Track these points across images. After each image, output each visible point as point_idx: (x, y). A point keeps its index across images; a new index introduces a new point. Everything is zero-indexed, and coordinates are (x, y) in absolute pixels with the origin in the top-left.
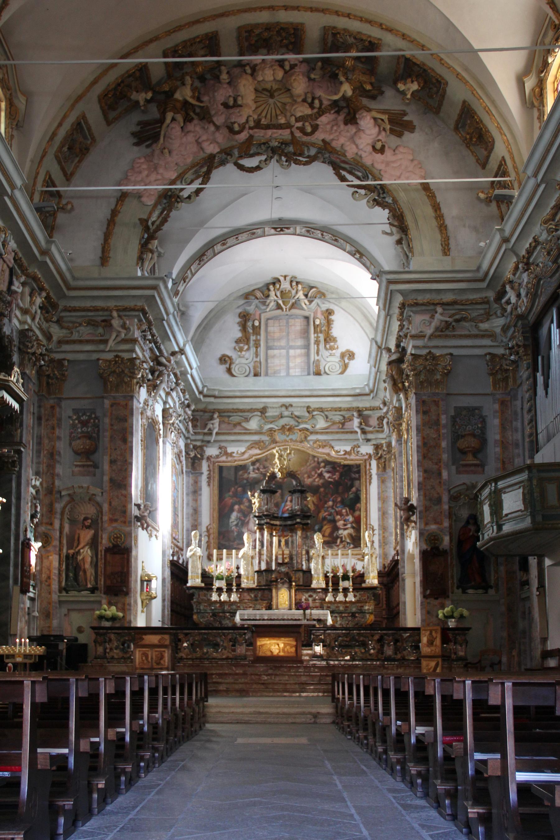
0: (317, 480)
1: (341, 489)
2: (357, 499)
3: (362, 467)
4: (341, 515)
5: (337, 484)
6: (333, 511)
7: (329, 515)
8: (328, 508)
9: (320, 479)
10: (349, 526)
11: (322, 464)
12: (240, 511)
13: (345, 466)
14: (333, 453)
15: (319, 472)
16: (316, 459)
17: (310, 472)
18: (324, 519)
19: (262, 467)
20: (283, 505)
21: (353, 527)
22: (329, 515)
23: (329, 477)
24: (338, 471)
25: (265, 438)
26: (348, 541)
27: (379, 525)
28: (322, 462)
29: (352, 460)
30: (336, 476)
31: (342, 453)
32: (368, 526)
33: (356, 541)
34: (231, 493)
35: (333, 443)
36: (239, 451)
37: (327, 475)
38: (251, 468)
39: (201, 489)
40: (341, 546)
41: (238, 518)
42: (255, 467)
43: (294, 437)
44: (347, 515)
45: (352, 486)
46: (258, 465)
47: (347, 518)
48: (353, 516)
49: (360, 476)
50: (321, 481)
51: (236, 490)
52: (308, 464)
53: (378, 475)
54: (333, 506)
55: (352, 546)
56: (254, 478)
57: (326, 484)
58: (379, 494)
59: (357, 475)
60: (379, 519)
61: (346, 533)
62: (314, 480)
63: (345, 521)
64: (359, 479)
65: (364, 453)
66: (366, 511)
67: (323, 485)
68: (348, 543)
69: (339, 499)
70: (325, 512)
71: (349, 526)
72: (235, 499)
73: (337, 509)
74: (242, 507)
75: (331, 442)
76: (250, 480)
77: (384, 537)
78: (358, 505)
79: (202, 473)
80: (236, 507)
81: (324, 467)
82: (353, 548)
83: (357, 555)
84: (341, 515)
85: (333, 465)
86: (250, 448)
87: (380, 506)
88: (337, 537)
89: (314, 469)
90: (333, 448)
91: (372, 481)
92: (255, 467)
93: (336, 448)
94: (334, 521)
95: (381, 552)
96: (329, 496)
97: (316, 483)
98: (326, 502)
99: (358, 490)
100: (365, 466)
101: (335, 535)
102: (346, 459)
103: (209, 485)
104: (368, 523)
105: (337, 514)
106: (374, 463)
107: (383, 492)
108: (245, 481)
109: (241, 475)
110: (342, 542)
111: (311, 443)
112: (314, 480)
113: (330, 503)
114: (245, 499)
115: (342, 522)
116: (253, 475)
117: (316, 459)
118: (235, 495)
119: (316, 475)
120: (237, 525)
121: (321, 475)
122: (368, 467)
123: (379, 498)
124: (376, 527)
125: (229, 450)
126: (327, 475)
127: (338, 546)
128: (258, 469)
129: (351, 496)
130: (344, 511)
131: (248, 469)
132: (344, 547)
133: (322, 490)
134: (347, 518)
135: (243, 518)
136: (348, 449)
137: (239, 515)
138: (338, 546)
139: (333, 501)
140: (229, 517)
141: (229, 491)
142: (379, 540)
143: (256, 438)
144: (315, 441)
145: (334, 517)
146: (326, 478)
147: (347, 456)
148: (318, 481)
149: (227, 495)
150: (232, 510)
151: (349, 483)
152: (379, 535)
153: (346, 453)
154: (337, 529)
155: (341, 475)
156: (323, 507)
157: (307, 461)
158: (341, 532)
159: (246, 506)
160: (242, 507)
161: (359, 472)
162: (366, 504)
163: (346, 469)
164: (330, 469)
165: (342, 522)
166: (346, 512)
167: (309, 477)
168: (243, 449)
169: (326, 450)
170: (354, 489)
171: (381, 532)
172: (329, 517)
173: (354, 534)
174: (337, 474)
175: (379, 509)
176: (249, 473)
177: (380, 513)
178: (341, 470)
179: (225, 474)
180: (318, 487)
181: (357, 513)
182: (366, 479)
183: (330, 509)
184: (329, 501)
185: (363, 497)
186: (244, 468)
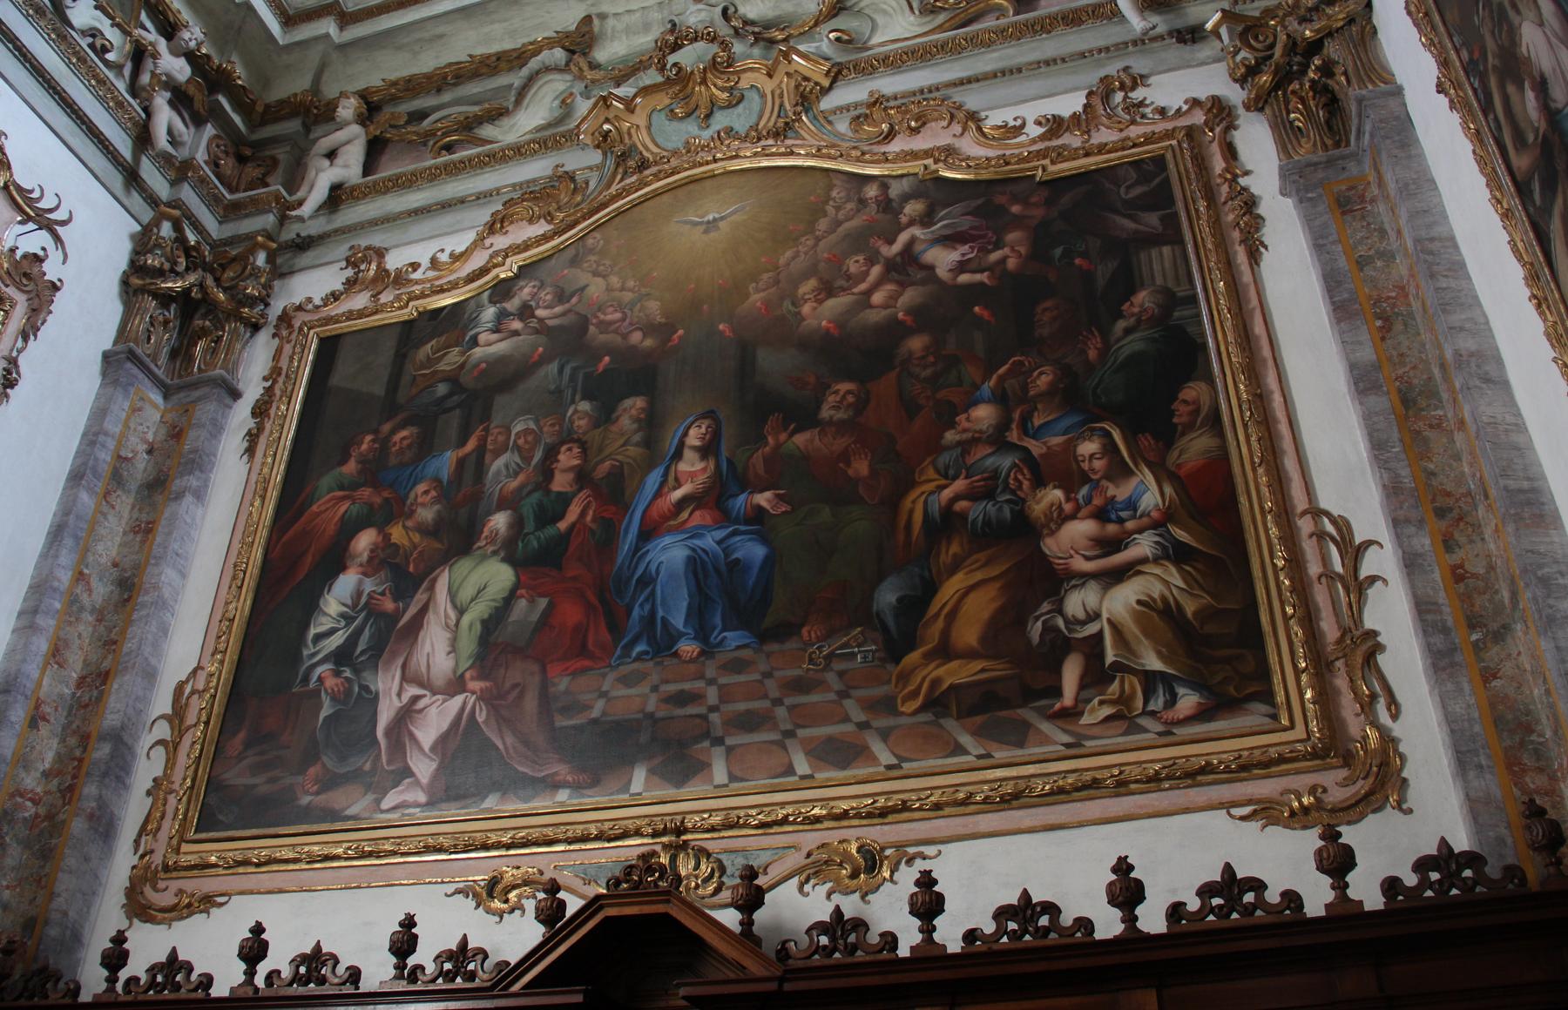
0: (877, 298)
1: (1046, 315)
2: (1181, 354)
3: (1185, 189)
4: (1070, 476)
5: (1015, 295)
6: (1006, 461)
7: (972, 495)
8: (966, 446)
9: (903, 285)
10: (1144, 545)
11: (913, 208)
12: (385, 560)
13: (1057, 185)
14: (971, 147)
15: (897, 247)
16: (872, 191)
17: (837, 262)
18: (945, 523)
19: (547, 296)
20: (653, 479)
21: (1176, 554)
22: (972, 495)
23: (962, 267)
24: (1017, 222)
25: (582, 160)
26: (1154, 663)
27: (1392, 491)
28: (906, 198)
29: (1102, 149)
30: (1012, 251)
31: (1034, 131)
32: (1305, 525)
33: (1220, 652)
34: (351, 467)
35: (971, 99)
36: (438, 247)
37: (943, 259)
38: (490, 313)
39: (199, 463)
40: (1097, 713)
41: (361, 608)
42: (512, 305)
43: (739, 119)
44: (1119, 471)
45: (1127, 283)
46: (526, 291)
47: (1121, 492)
48: (1162, 472)
49: (1172, 221)
50: (910, 296)
51: (384, 443)
52: (823, 225)
53: (1296, 179)
54: (1003, 426)
55: (1188, 701)
56: (502, 360)
57: (945, 309)
58: (1332, 282)
59: (1153, 220)
60: (1377, 446)
61: (1122, 601)
62: (865, 300)
63: (1101, 515)
64: (1171, 234)
65: (1174, 101)
66: (1266, 422)
67: (922, 318)
68: (1150, 680)
69: (1043, 380)
70: (948, 476)
71: (1144, 545)
72: (366, 492)
73: (1036, 448)
74: (397, 533)
75: (958, 96)
76: (466, 379)
77: (1458, 575)
78: (1193, 391)
79: (236, 395)
80: (365, 541)
81: (926, 220)
82: (1202, 715)
83: (1245, 768)
84: (1070, 476)
85: (984, 202)
86: (496, 225)
87: (1367, 354)
88: (1059, 645)
89: (859, 242)
90: (974, 118)
91: (1268, 234)
92: (512, 305)
93: (994, 118)
94: (1023, 531)
95: (1468, 701)
96: (971, 372)
97: (874, 316)
98: (948, 415)
99: (1178, 301)
100: (1201, 163)
101: (1035, 630)
102: (1060, 154)
103: (250, 451)
104: (1300, 502)
105: (1039, 482)
106: (1257, 143)
107: (1361, 263)
108: (442, 389)
109: (430, 361)
110: (1096, 676)
111: (843, 126)
112: (865, 300)
113: (984, 415)
114: (421, 488)
115: (1081, 529)
116: (490, 347)
117: (872, 191)
118: (373, 472)
119: (876, 271)
120: (342, 657)
121: (906, 266)
122: (1218, 164)
123: (1342, 310)
124: (1366, 512)
125: (394, 261)
126: (943, 259)
127: (1069, 715)
128: (526, 312)
129: (1133, 345)
130: (1088, 447)
131: (474, 320)
132: (1123, 717)
133: (916, 344)
134: (1121, 492)
135: (389, 605)
136: (1070, 104)
137: (369, 586)
138: (1069, 715)
139: (1001, 398)
140: (311, 607)
141: (343, 462)
142: (1423, 608)
143: (536, 169)
144: (862, 115)
145: (1019, 505)
146: (942, 272)
147: (1073, 140)
148: (887, 301)
149: (326, 481)
150: (335, 562)
151: (1103, 272)
152: (1411, 564)
153: (1056, 125)
154: (1052, 581)
155: (1041, 240)
156: (934, 447)
157: (818, 211)
158: (1077, 602)
159: (423, 530)
160: (397, 533)
161: (1161, 198)
162: (1253, 370)
163: (1066, 200)
164: (966, 223)
165: (1081, 529)
166: (1110, 449)
167: (828, 290)
168: (460, 242)
169: (935, 136)
170: (1143, 299)
171: (1424, 542)
172: (976, 511)
173: (1190, 607)
174: (1012, 237)
175: (1363, 381)
176: (474, 342)
177: (1380, 402)
178: (1038, 213)
179: (342, 375)
180: (893, 331)
181: (1194, 448)
182: (1216, 223)
183: (982, 451)
184: (975, 403)
185: (1218, 338)
186: (451, 323)
